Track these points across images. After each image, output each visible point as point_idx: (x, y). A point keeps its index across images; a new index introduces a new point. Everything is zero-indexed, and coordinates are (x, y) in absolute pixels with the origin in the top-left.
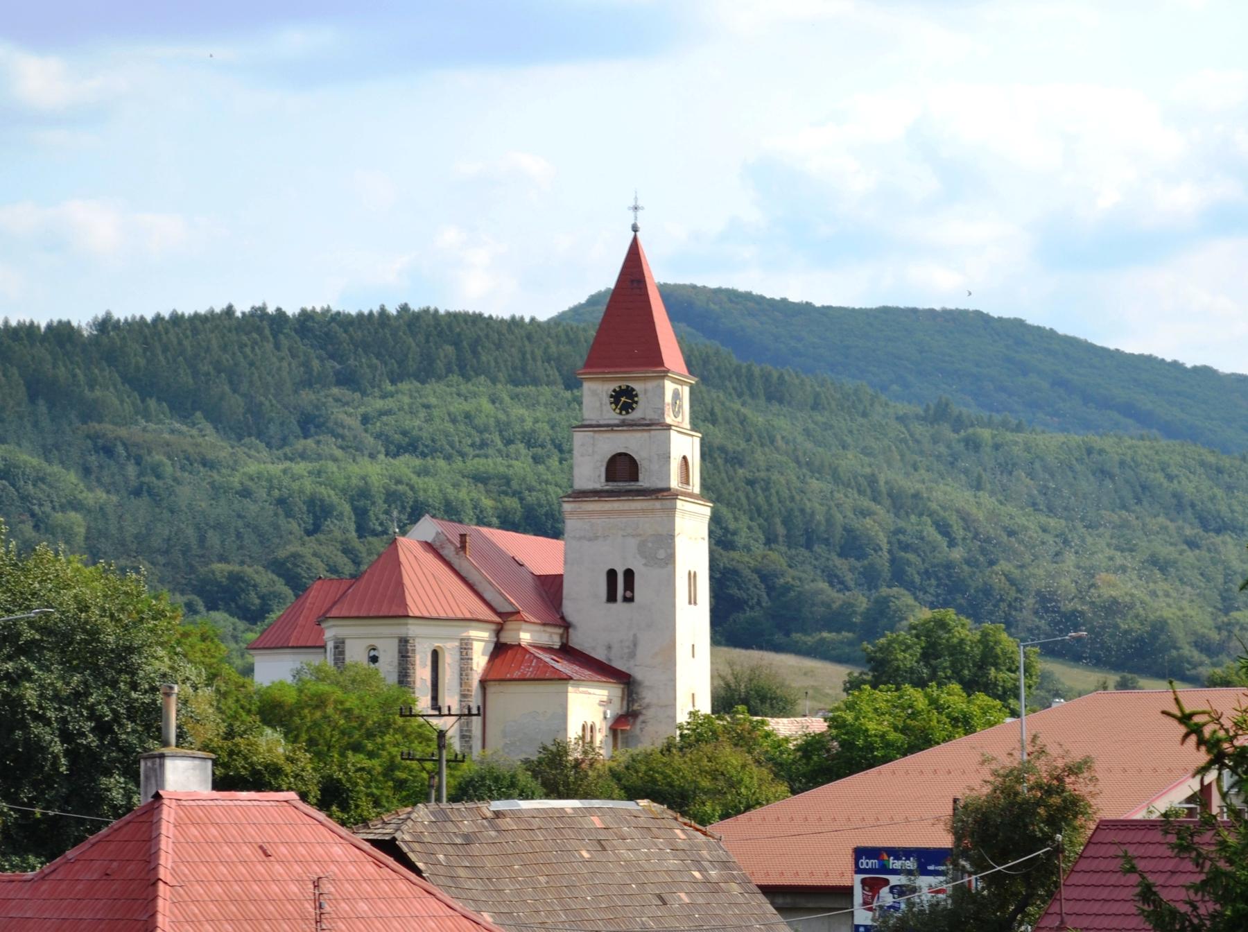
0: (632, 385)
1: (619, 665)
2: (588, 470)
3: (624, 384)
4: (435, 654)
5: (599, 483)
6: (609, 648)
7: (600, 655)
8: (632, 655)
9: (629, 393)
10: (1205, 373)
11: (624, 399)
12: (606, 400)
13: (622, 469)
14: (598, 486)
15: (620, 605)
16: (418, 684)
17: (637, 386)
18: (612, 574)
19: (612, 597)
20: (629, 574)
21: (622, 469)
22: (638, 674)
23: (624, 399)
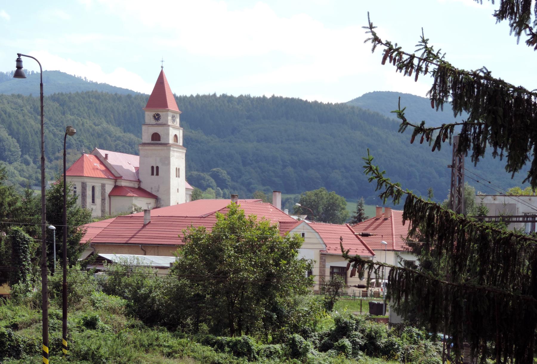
0: (159, 113)
1: (154, 193)
2: (146, 137)
3: (157, 113)
4: (93, 188)
5: (149, 140)
6: (152, 188)
7: (149, 190)
8: (158, 191)
9: (158, 115)
10: (416, 96)
11: (157, 117)
12: (152, 117)
13: (156, 137)
14: (149, 142)
15: (155, 176)
16: (88, 195)
17: (160, 113)
18: (153, 167)
19: (153, 174)
20: (157, 168)
21: (156, 137)
22: (159, 196)
23: (157, 117)
